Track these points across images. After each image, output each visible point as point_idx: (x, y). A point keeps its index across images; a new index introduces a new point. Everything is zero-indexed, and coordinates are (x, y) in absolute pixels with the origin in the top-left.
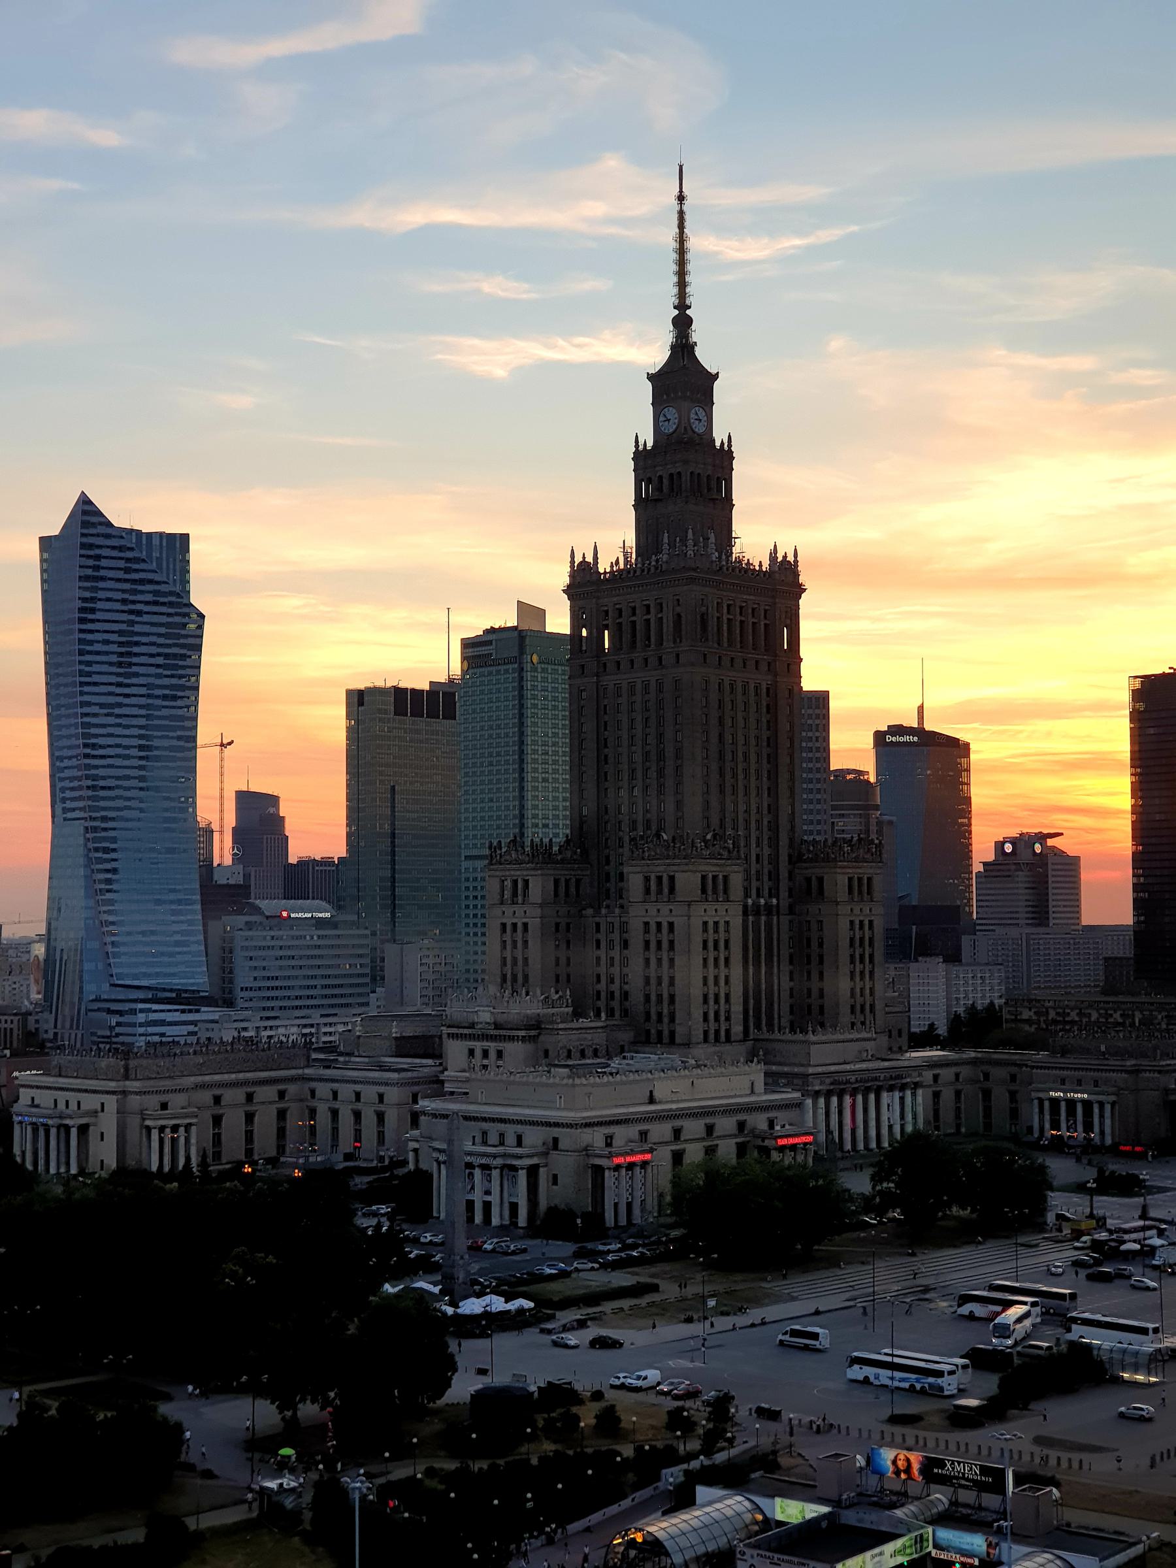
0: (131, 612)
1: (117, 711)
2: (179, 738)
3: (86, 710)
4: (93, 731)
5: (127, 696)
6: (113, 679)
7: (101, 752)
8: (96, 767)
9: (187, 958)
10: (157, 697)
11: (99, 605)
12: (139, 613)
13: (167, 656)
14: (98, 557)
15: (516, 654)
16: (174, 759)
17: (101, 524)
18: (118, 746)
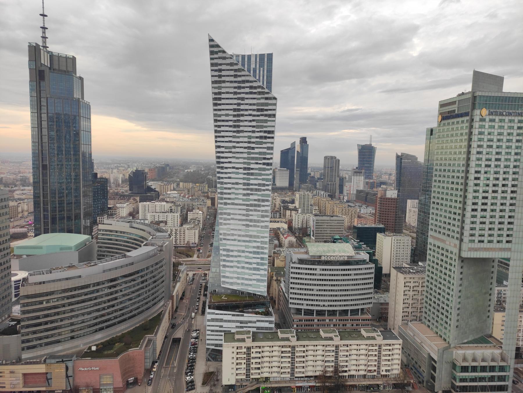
0: (239, 99)
1: (233, 150)
2: (264, 164)
3: (219, 150)
4: (222, 160)
5: (238, 142)
6: (231, 134)
7: (225, 171)
8: (222, 178)
9: (258, 277)
10: (253, 143)
11: (223, 96)
12: (243, 99)
13: (257, 121)
14: (220, 70)
15: (470, 110)
16: (260, 175)
17: (220, 52)
18: (233, 168)
